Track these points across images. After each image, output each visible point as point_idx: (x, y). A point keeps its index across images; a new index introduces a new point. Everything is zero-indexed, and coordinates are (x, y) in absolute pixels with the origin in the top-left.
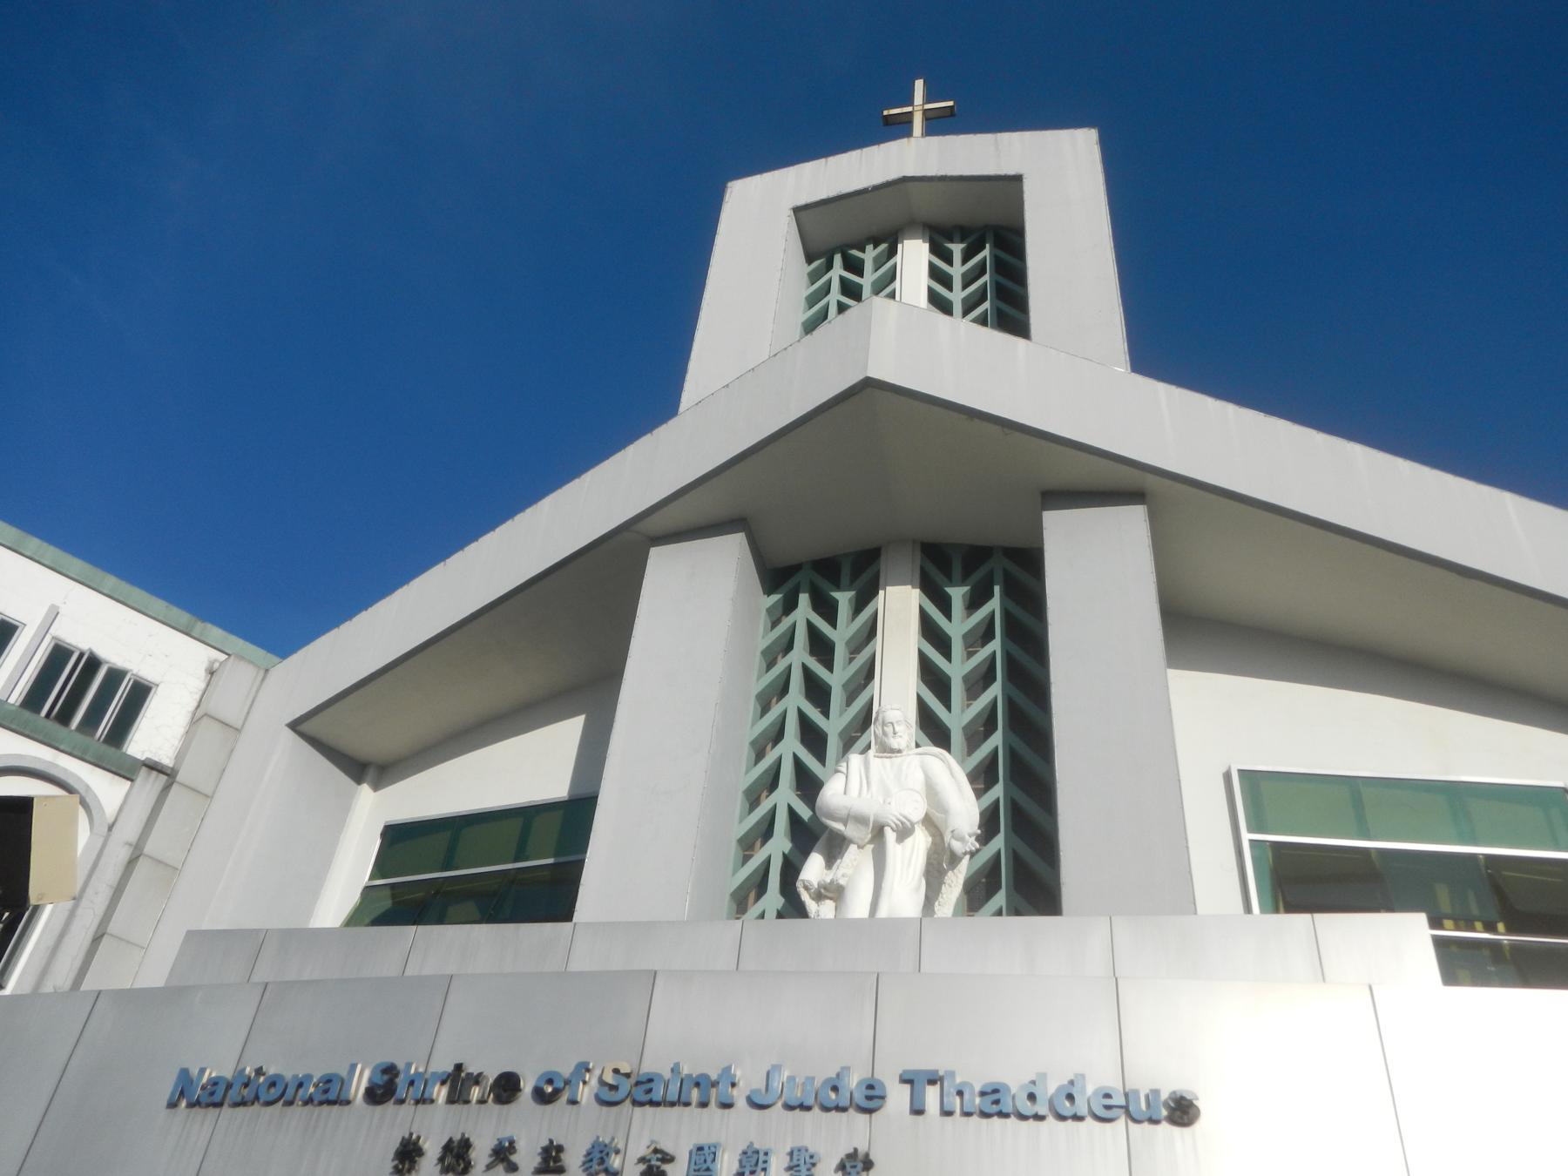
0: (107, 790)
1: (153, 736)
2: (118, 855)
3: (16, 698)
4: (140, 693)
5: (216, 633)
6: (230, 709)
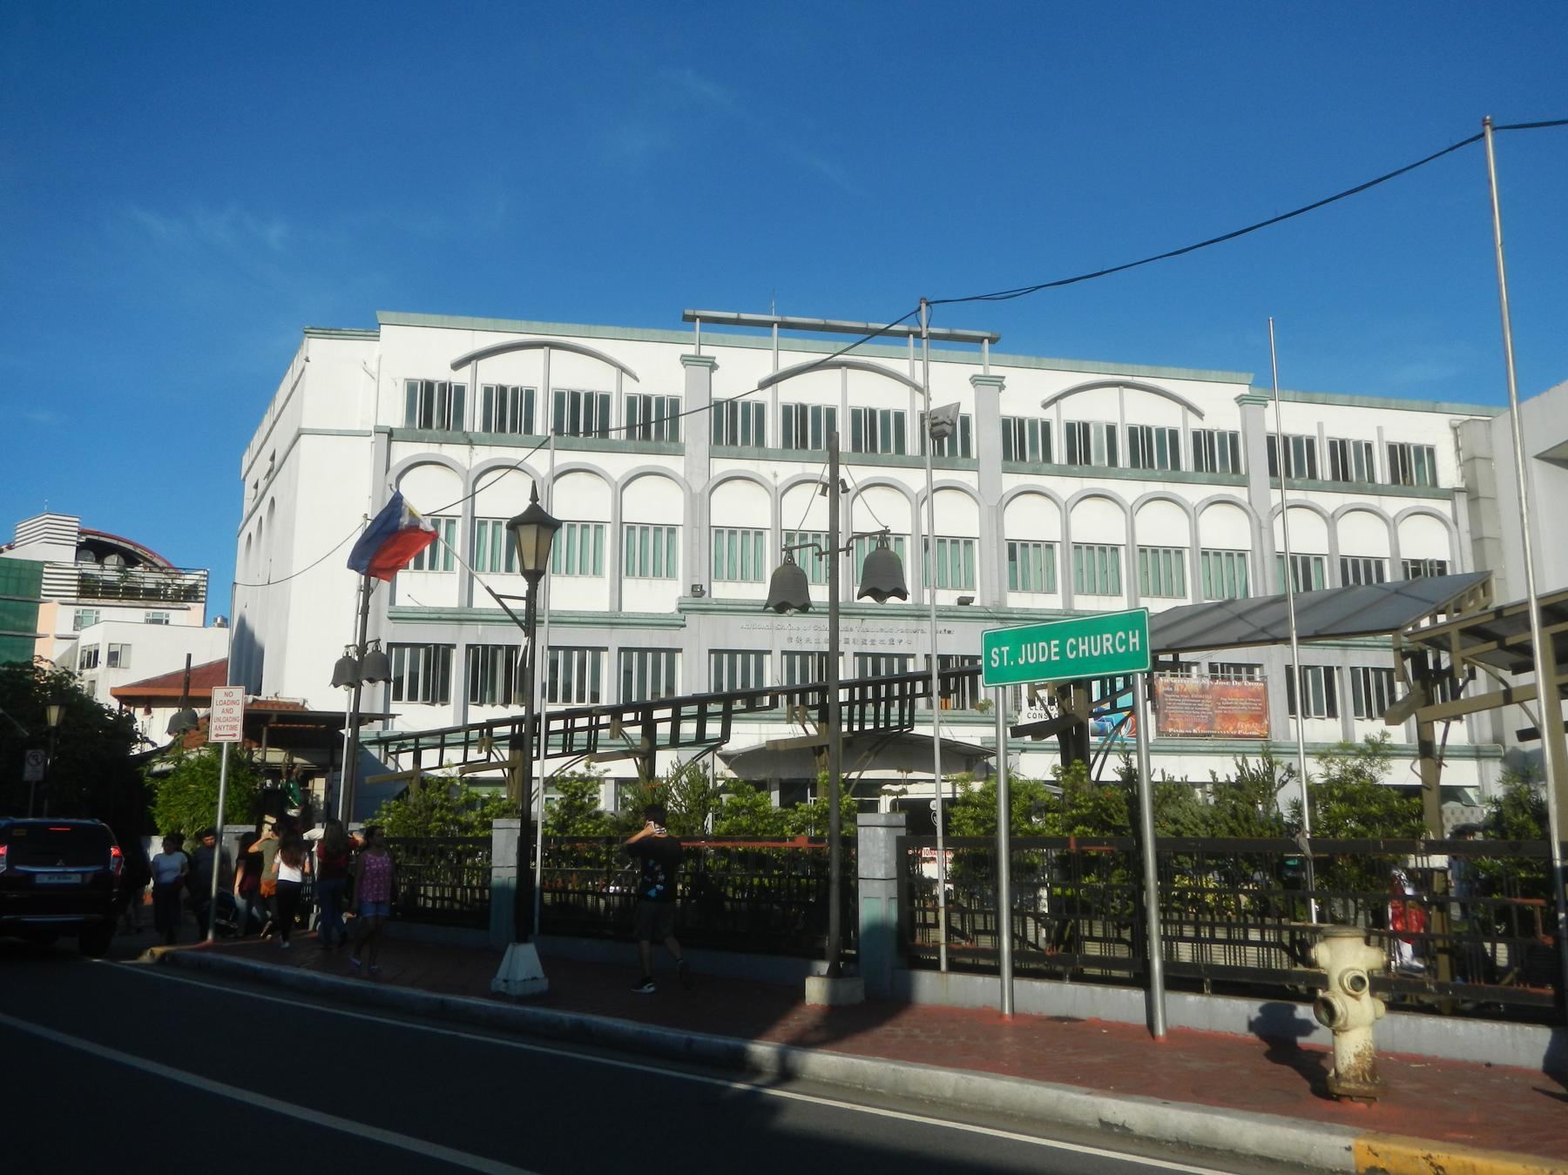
0: (1444, 507)
1: (1449, 473)
2: (1466, 539)
3: (1388, 480)
4: (1431, 451)
5: (1446, 405)
6: (1481, 451)
